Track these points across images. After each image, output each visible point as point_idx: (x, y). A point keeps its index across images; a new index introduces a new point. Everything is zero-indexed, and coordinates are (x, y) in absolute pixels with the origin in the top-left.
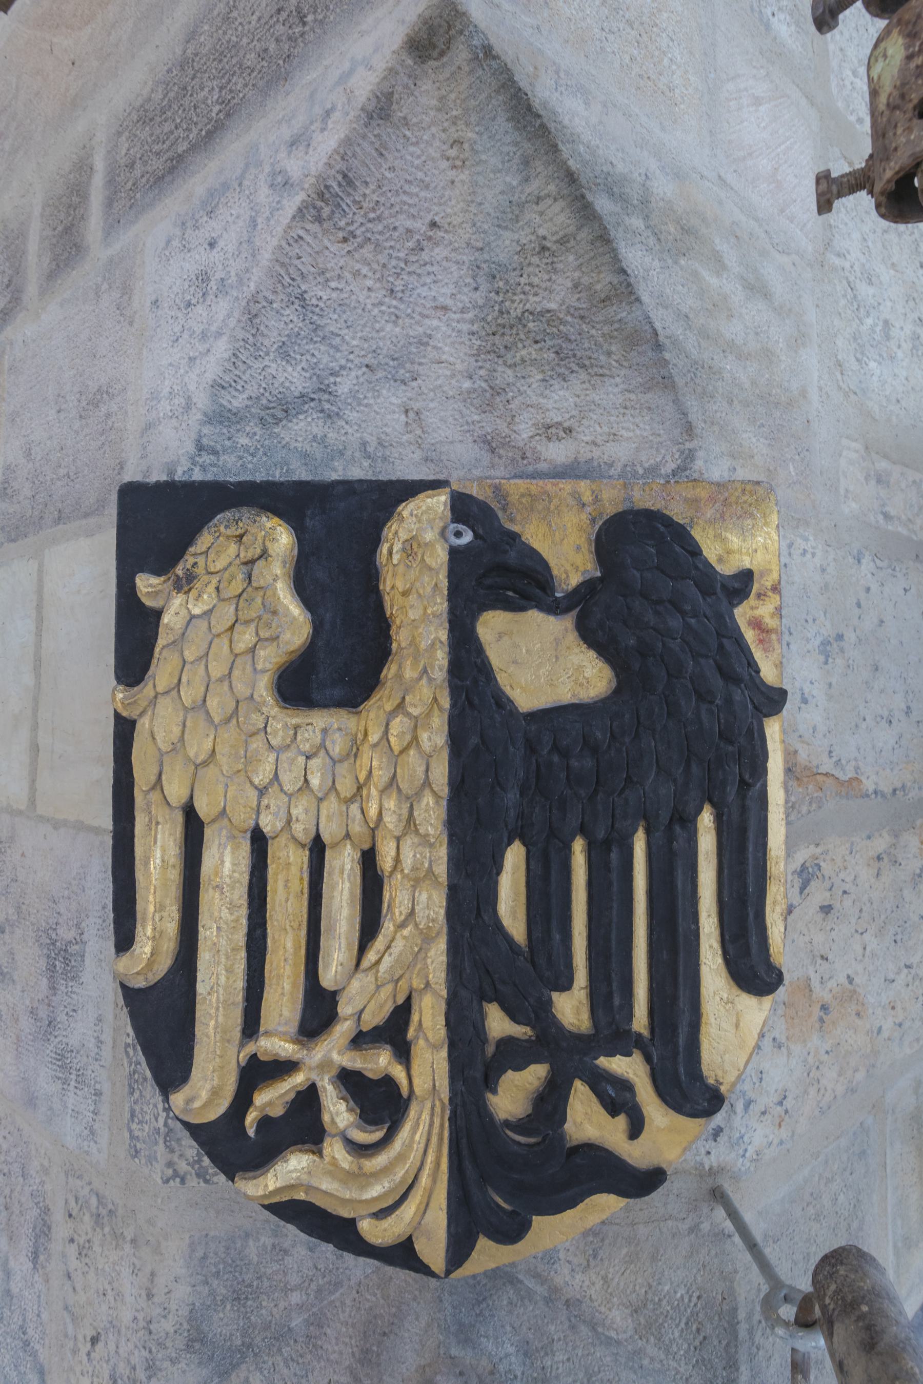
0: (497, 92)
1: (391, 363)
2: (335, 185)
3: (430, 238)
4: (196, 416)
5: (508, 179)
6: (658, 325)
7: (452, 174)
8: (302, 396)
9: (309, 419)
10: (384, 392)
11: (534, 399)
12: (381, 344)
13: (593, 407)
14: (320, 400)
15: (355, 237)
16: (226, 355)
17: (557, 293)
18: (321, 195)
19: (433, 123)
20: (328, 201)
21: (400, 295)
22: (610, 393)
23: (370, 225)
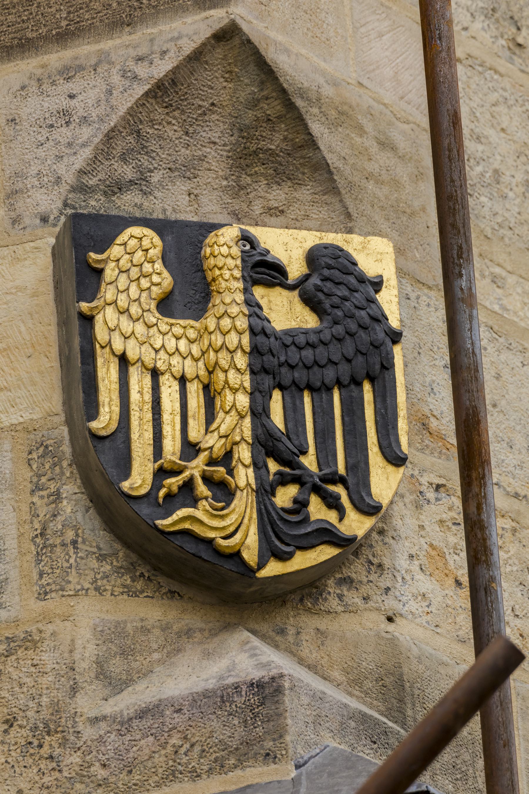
0: (252, 55)
1: (183, 168)
2: (167, 84)
3: (210, 110)
4: (64, 188)
5: (252, 89)
6: (329, 162)
7: (225, 84)
8: (131, 181)
9: (133, 194)
10: (178, 183)
11: (263, 194)
12: (178, 158)
13: (295, 200)
14: (140, 184)
15: (172, 106)
16: (90, 157)
17: (275, 141)
18: (159, 87)
19: (219, 64)
20: (163, 91)
21: (191, 135)
22: (305, 194)
23: (181, 102)
